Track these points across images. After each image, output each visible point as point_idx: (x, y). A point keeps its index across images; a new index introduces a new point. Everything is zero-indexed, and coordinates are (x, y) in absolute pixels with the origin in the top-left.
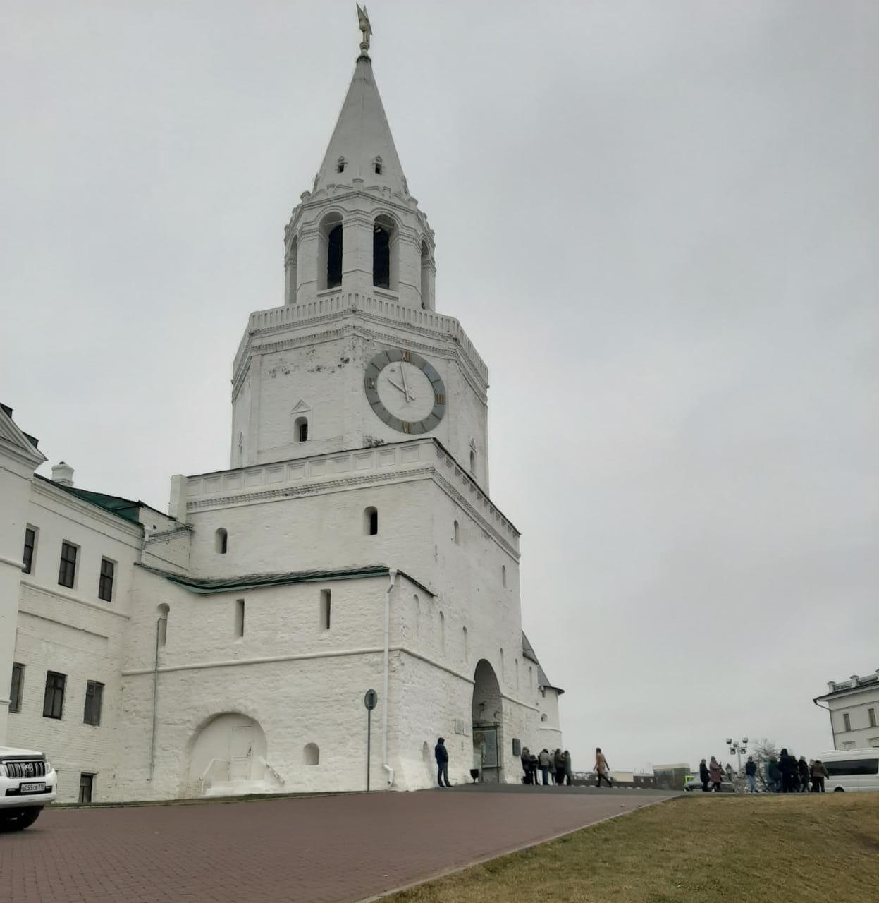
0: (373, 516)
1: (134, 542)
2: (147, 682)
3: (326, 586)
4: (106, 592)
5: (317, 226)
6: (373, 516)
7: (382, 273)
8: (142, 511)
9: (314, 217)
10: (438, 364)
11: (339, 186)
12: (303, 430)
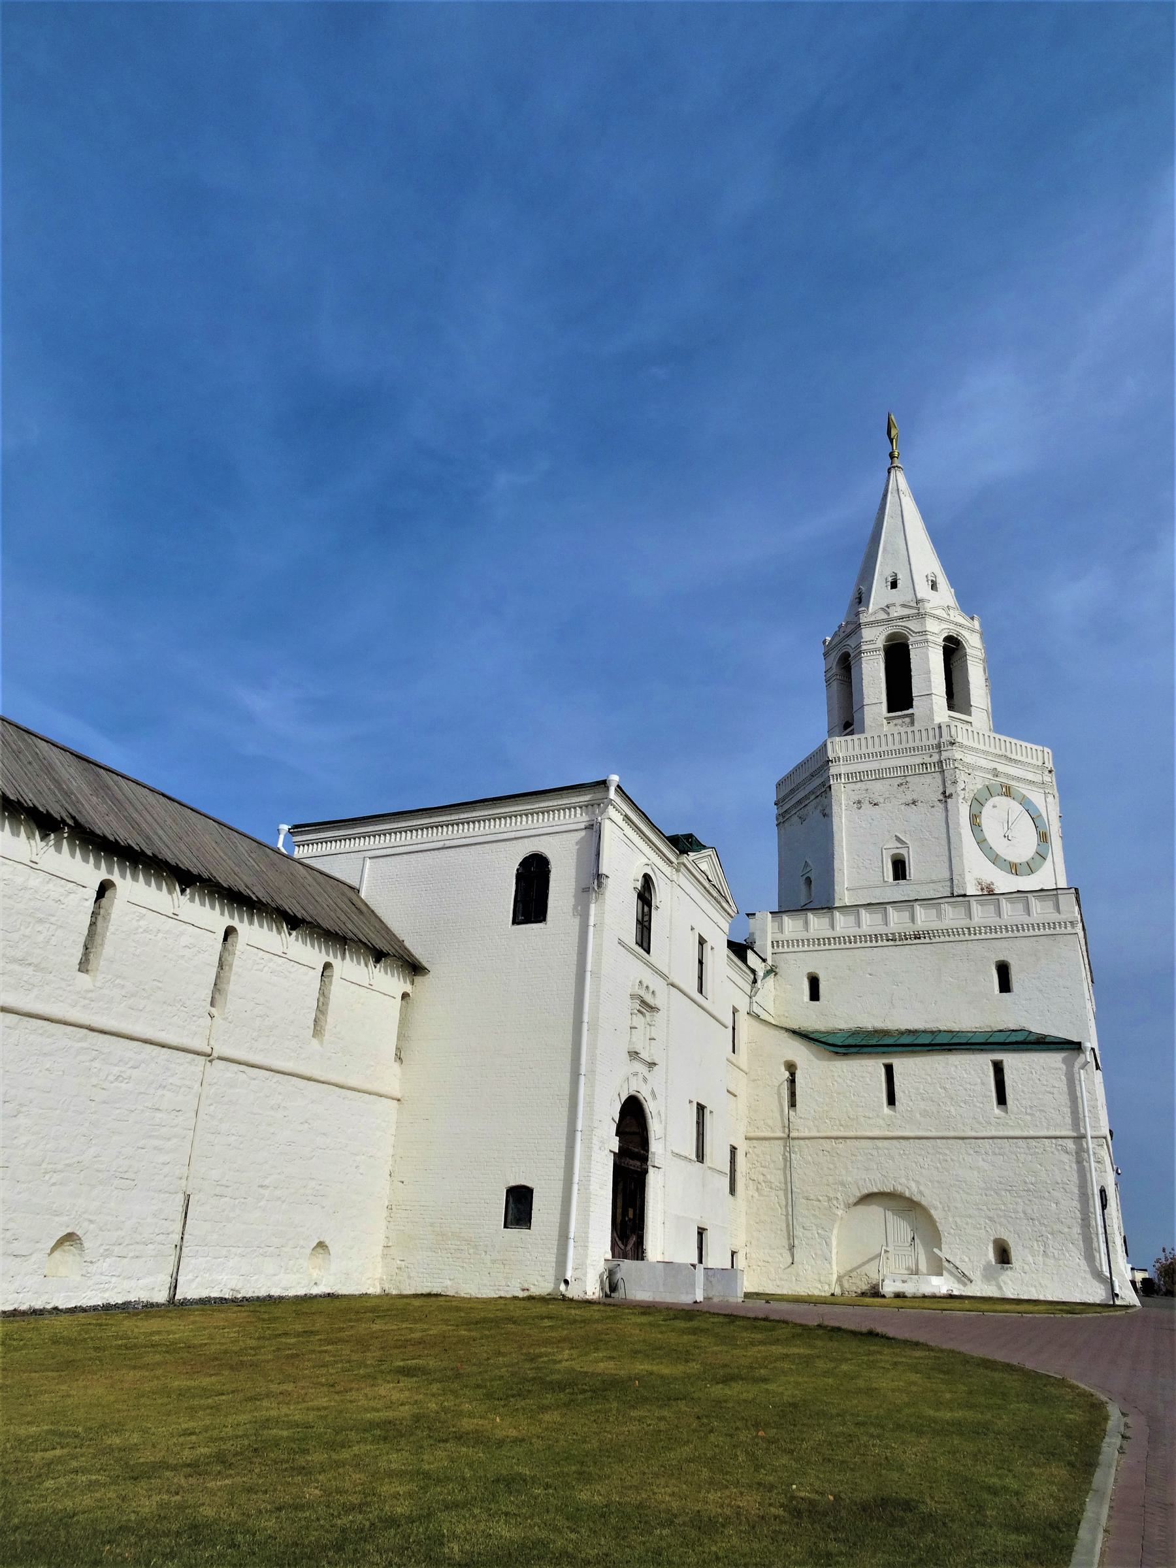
0: (1003, 970)
1: (748, 988)
2: (778, 1147)
3: (998, 1056)
6: (1003, 970)
9: (874, 639)
12: (900, 869)
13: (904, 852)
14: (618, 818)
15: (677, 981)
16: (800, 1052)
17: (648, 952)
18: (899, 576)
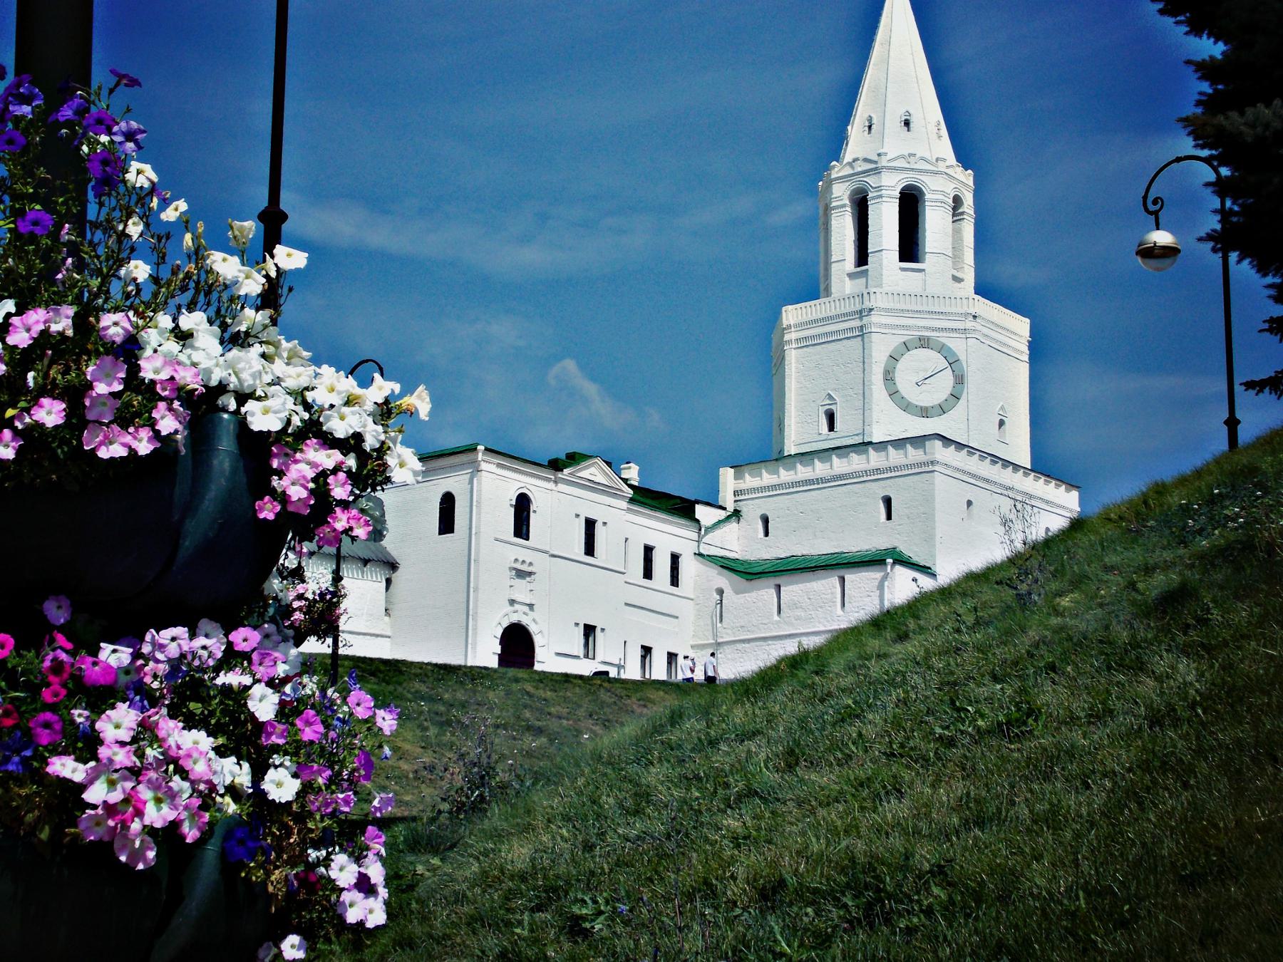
0: (888, 502)
1: (695, 536)
3: (841, 572)
4: (675, 581)
5: (847, 202)
6: (888, 502)
7: (910, 249)
8: (698, 508)
10: (956, 345)
11: (866, 160)
13: (833, 407)
14: (493, 468)
15: (556, 553)
16: (722, 580)
17: (527, 539)
18: (874, 121)
